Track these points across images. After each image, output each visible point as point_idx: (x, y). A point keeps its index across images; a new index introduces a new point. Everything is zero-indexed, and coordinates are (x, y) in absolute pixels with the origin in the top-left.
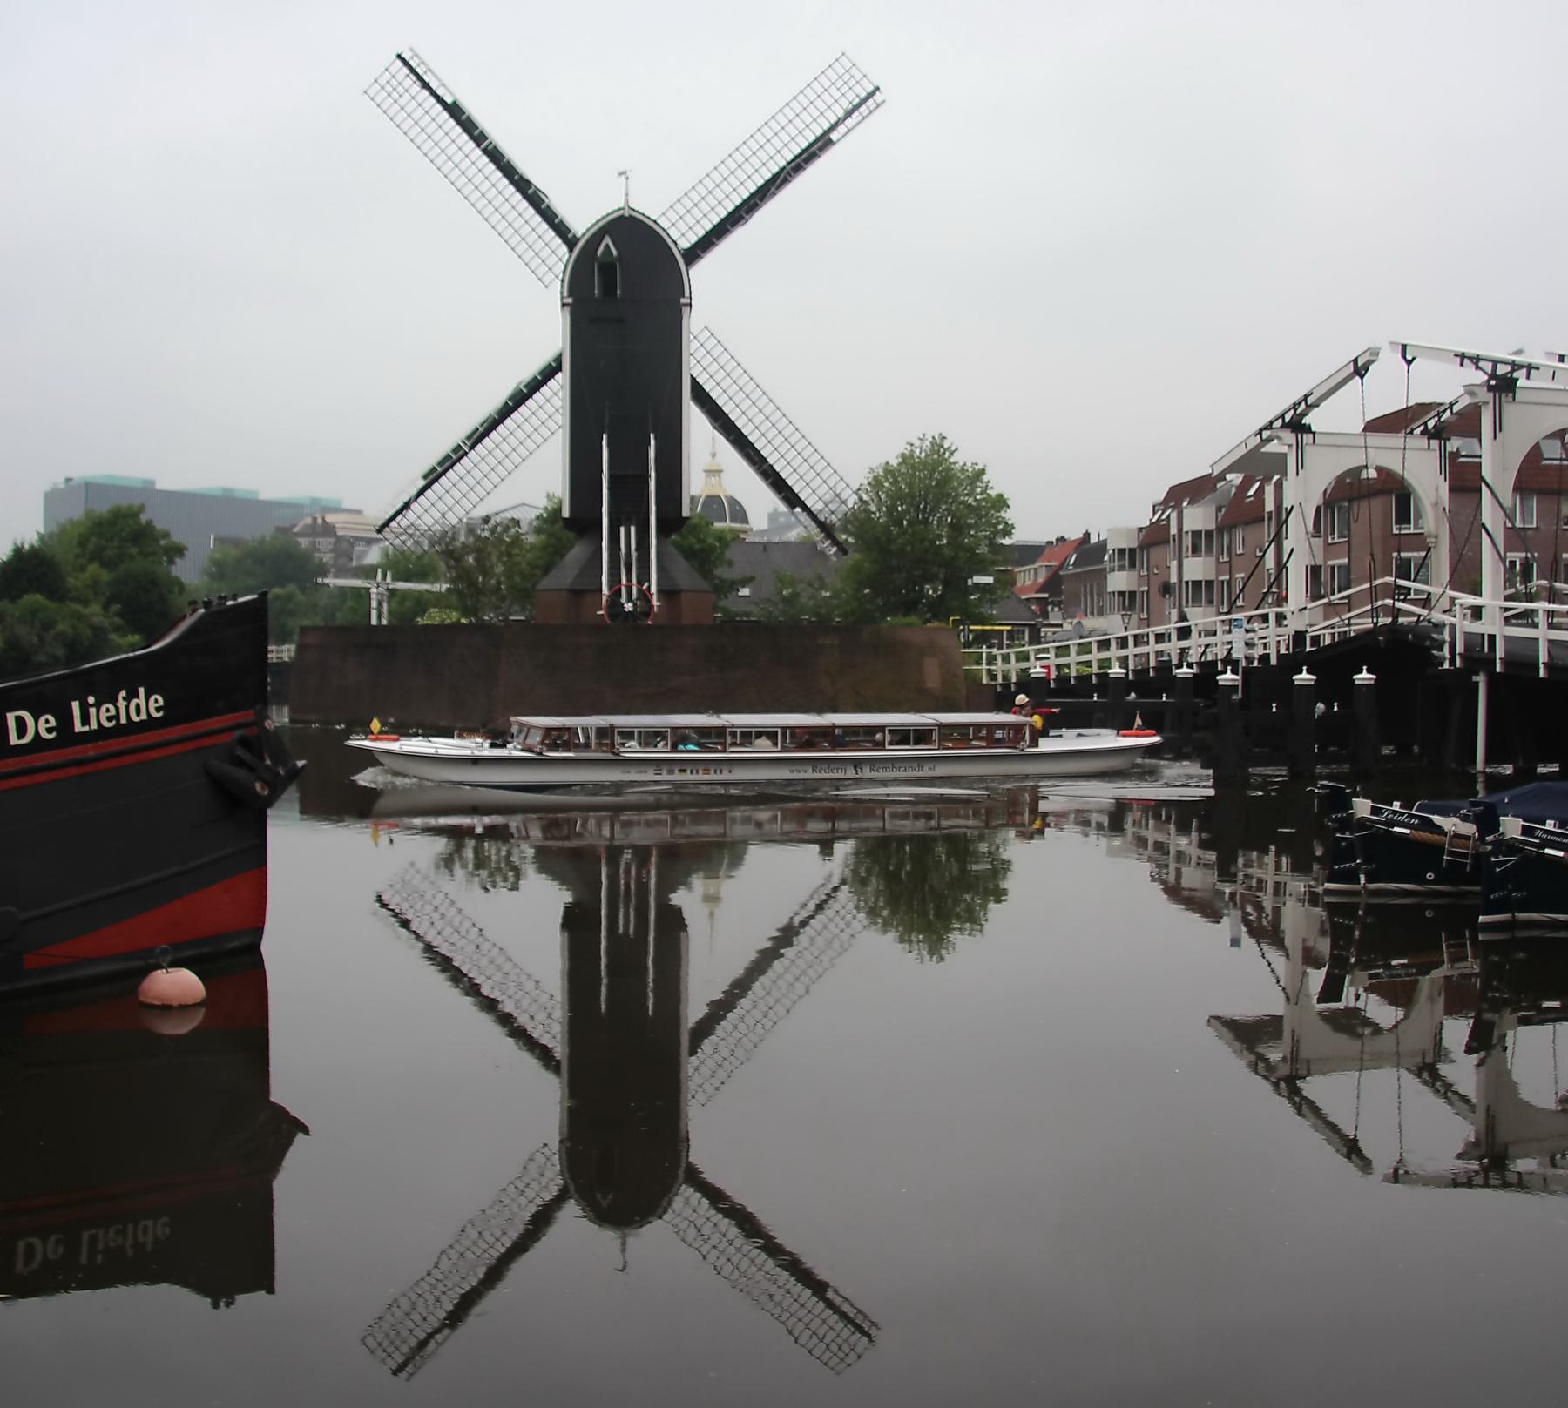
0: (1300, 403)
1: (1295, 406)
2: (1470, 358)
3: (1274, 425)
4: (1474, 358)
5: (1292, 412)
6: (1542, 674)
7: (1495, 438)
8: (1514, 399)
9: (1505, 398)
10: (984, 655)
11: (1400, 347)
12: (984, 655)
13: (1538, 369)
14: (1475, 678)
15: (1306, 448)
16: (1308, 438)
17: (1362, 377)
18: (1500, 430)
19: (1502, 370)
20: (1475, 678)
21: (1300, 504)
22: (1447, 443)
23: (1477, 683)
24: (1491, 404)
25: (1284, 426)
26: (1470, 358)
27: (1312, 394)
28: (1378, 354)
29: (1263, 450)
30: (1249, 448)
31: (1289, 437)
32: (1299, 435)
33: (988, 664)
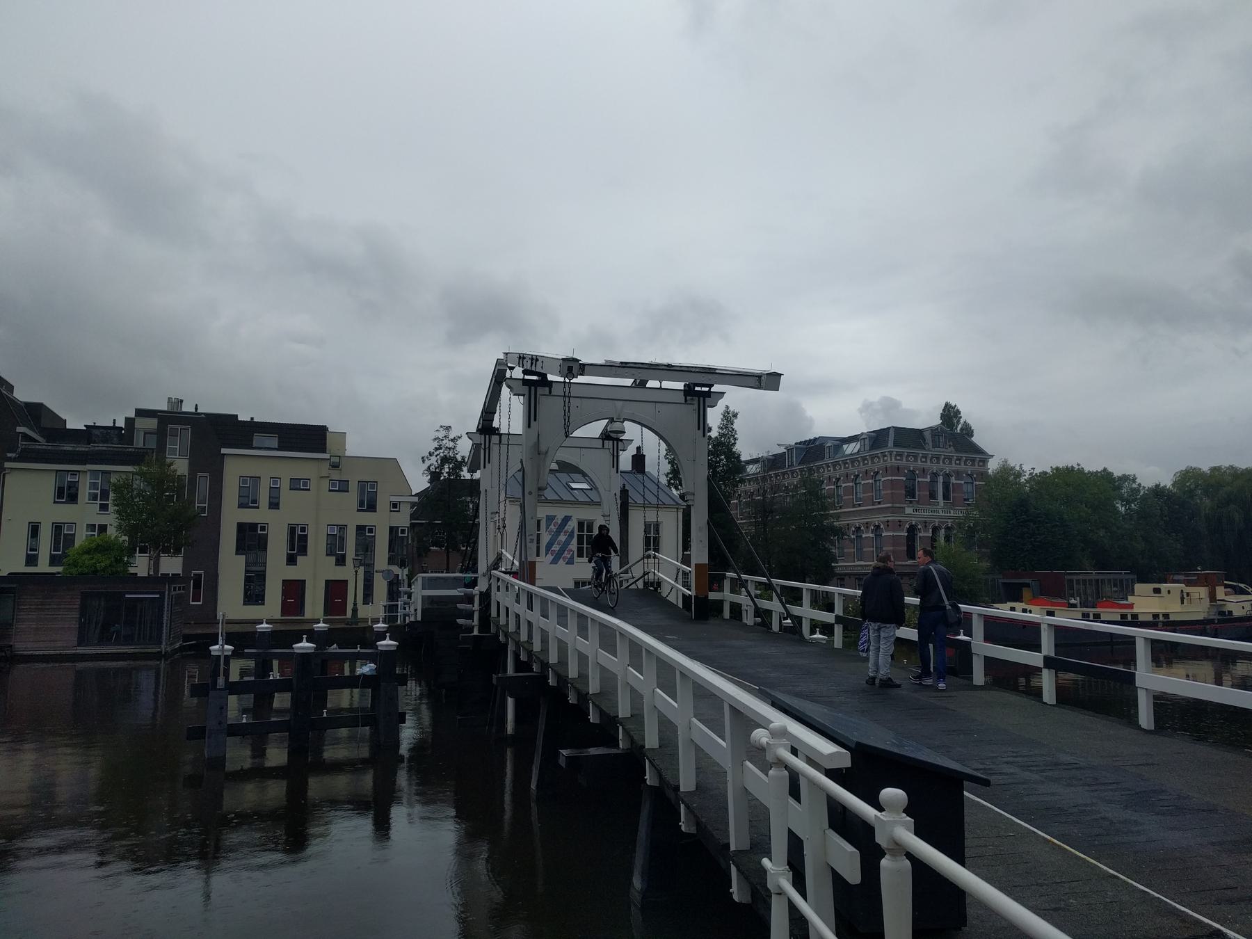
7: (529, 426)
8: (550, 392)
9: (540, 390)
22: (620, 443)
32: (487, 436)
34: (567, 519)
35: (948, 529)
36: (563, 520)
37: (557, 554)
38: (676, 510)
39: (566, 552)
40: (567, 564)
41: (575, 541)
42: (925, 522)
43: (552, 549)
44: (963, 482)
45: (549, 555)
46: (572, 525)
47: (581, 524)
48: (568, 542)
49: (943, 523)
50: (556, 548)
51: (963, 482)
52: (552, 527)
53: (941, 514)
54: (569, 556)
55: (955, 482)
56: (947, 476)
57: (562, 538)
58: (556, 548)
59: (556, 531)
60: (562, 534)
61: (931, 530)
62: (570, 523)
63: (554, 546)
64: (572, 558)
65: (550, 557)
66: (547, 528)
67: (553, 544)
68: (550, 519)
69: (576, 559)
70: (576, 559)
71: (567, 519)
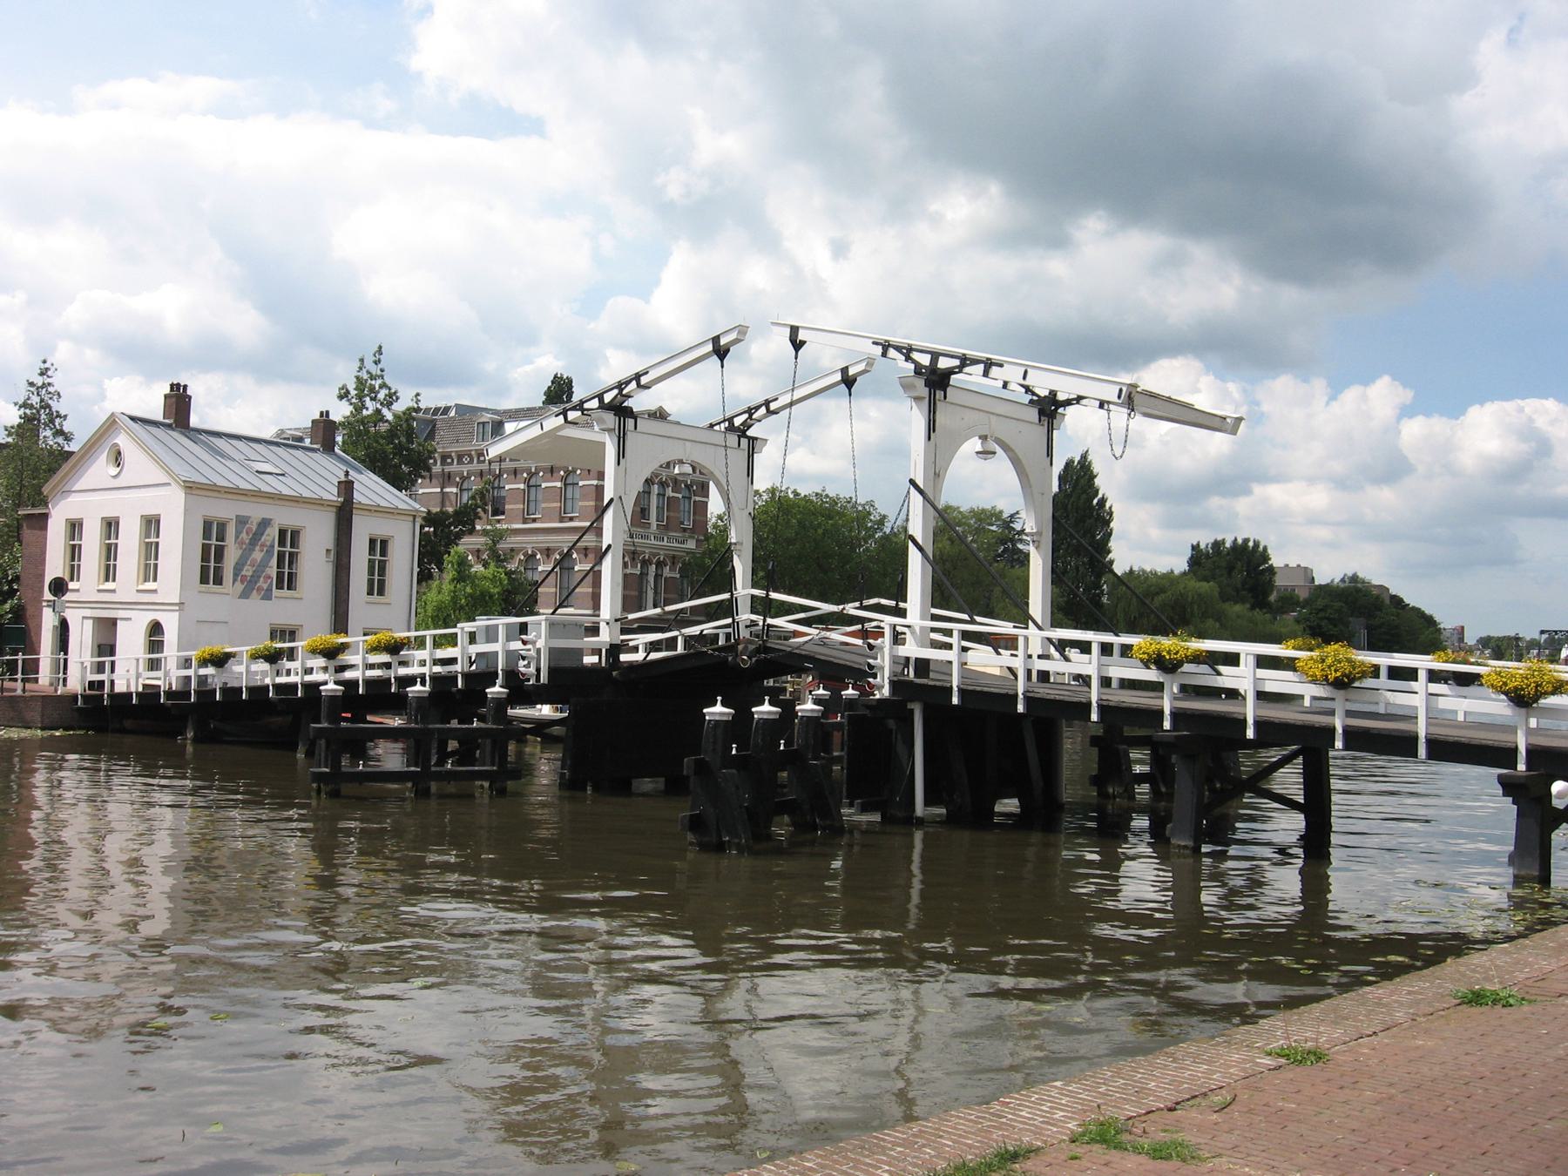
0: (630, 381)
1: (620, 386)
2: (898, 349)
3: (586, 406)
4: (904, 348)
5: (615, 392)
6: (955, 701)
8: (945, 397)
9: (940, 394)
10: (20, 663)
11: (788, 330)
12: (20, 663)
13: (1001, 366)
14: (910, 706)
15: (629, 436)
16: (630, 422)
17: (722, 360)
18: (934, 431)
19: (944, 363)
20: (910, 706)
21: (620, 498)
23: (912, 711)
24: (927, 399)
25: (603, 406)
26: (898, 349)
27: (647, 373)
28: (745, 333)
29: (559, 434)
30: (545, 430)
31: (610, 419)
33: (22, 674)
34: (265, 523)
35: (660, 564)
36: (259, 524)
37: (250, 581)
38: (411, 519)
39: (262, 579)
40: (262, 599)
41: (274, 561)
42: (674, 557)
43: (244, 573)
44: (680, 496)
45: (238, 583)
46: (272, 534)
47: (282, 533)
48: (264, 564)
49: (655, 555)
50: (248, 571)
51: (680, 496)
52: (244, 535)
53: (653, 542)
54: (265, 586)
55: (672, 494)
56: (663, 484)
57: (258, 555)
58: (248, 571)
59: (250, 544)
60: (258, 548)
61: (639, 565)
62: (269, 530)
63: (246, 568)
64: (269, 590)
65: (240, 587)
66: (237, 537)
67: (243, 565)
68: (242, 521)
69: (275, 592)
70: (275, 592)
71: (265, 523)
